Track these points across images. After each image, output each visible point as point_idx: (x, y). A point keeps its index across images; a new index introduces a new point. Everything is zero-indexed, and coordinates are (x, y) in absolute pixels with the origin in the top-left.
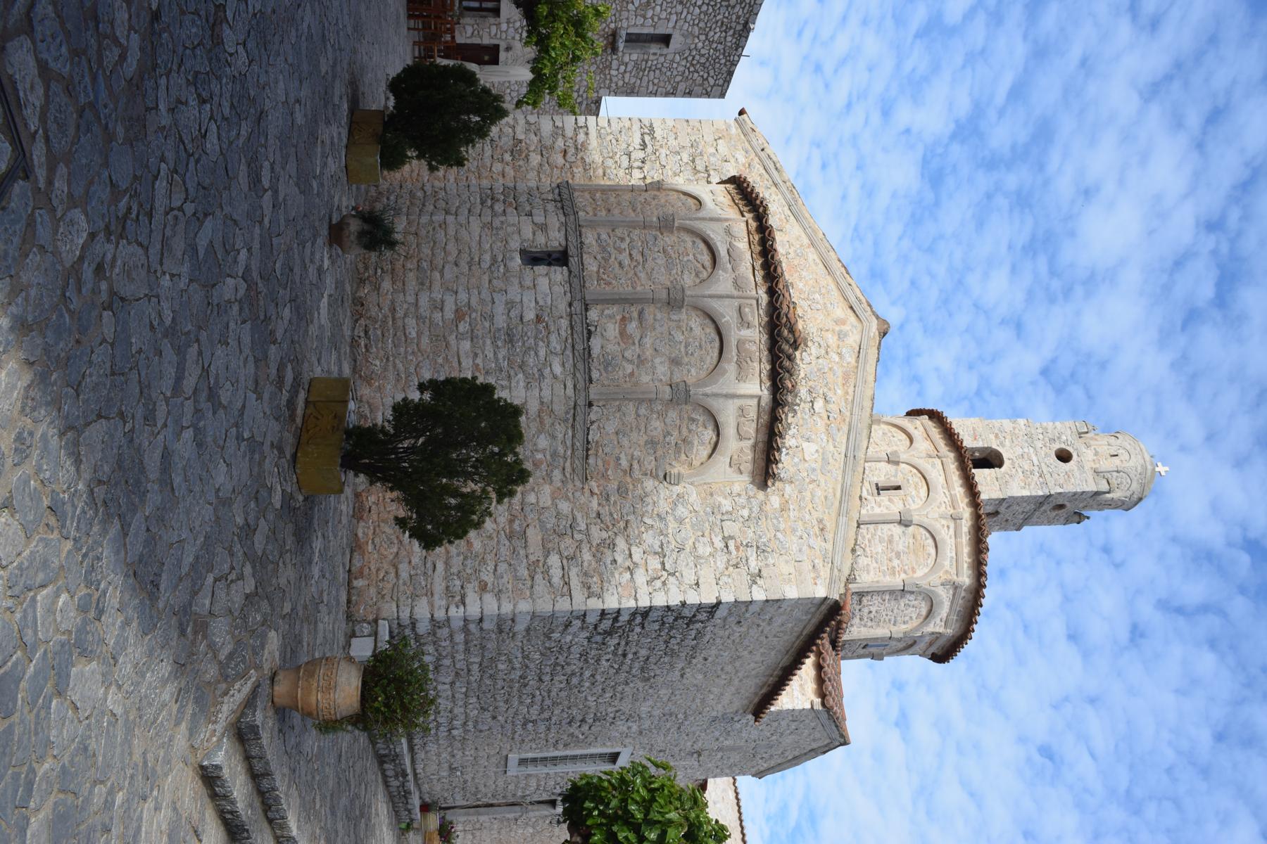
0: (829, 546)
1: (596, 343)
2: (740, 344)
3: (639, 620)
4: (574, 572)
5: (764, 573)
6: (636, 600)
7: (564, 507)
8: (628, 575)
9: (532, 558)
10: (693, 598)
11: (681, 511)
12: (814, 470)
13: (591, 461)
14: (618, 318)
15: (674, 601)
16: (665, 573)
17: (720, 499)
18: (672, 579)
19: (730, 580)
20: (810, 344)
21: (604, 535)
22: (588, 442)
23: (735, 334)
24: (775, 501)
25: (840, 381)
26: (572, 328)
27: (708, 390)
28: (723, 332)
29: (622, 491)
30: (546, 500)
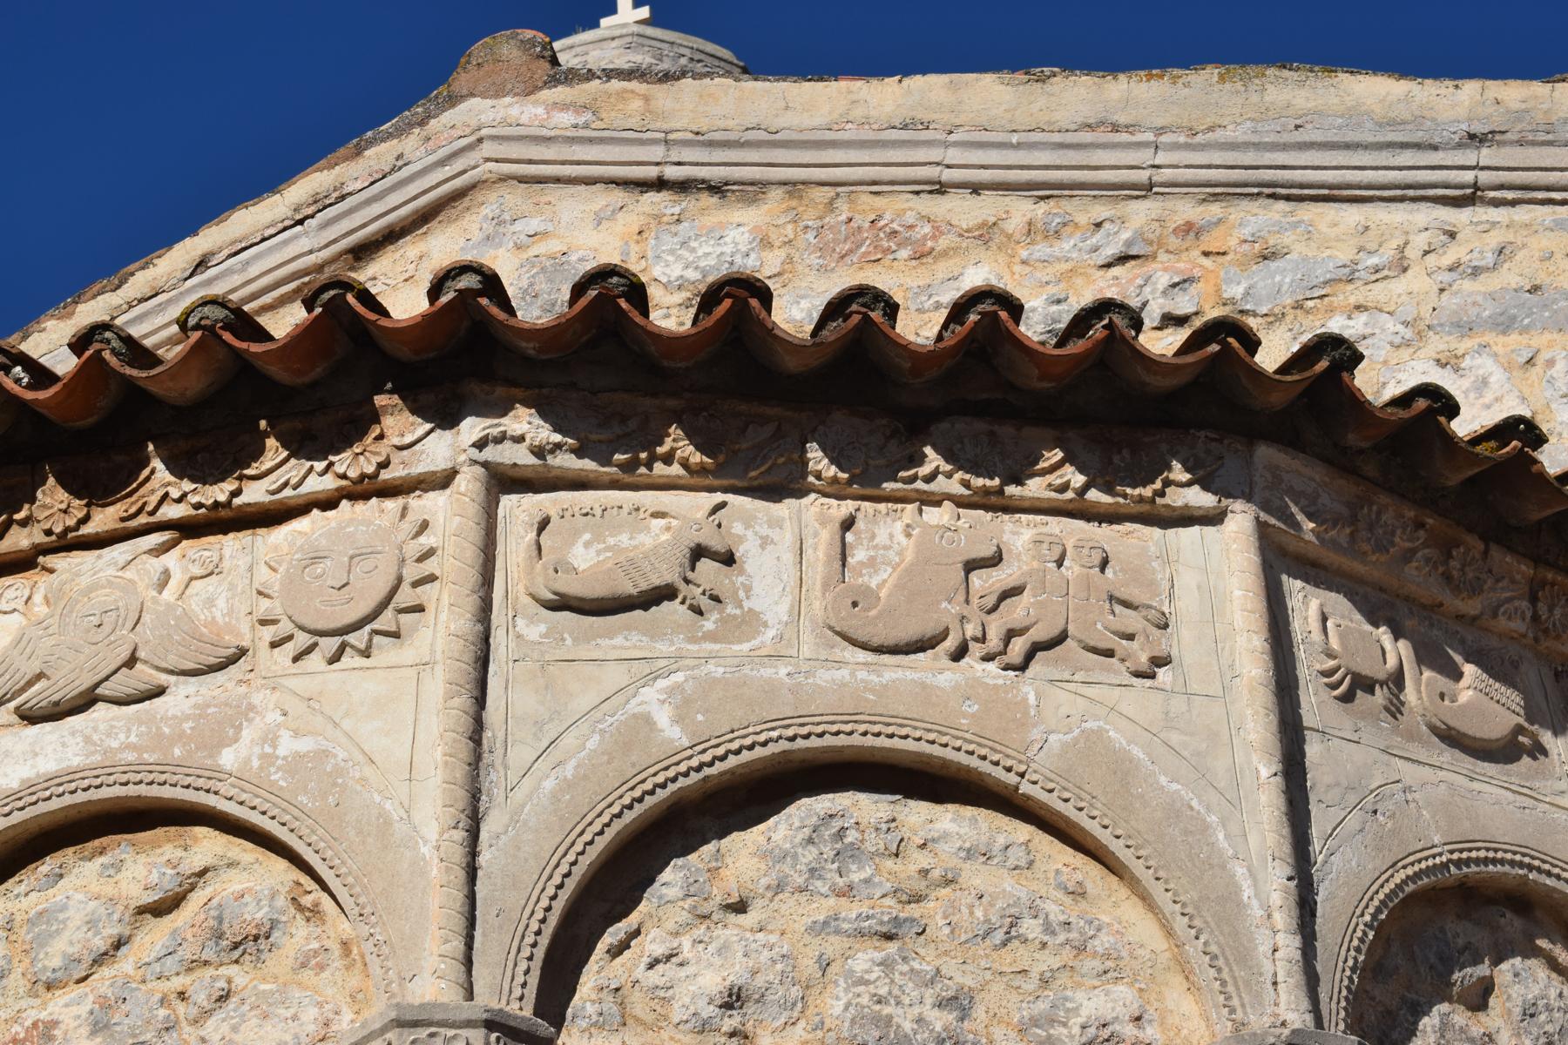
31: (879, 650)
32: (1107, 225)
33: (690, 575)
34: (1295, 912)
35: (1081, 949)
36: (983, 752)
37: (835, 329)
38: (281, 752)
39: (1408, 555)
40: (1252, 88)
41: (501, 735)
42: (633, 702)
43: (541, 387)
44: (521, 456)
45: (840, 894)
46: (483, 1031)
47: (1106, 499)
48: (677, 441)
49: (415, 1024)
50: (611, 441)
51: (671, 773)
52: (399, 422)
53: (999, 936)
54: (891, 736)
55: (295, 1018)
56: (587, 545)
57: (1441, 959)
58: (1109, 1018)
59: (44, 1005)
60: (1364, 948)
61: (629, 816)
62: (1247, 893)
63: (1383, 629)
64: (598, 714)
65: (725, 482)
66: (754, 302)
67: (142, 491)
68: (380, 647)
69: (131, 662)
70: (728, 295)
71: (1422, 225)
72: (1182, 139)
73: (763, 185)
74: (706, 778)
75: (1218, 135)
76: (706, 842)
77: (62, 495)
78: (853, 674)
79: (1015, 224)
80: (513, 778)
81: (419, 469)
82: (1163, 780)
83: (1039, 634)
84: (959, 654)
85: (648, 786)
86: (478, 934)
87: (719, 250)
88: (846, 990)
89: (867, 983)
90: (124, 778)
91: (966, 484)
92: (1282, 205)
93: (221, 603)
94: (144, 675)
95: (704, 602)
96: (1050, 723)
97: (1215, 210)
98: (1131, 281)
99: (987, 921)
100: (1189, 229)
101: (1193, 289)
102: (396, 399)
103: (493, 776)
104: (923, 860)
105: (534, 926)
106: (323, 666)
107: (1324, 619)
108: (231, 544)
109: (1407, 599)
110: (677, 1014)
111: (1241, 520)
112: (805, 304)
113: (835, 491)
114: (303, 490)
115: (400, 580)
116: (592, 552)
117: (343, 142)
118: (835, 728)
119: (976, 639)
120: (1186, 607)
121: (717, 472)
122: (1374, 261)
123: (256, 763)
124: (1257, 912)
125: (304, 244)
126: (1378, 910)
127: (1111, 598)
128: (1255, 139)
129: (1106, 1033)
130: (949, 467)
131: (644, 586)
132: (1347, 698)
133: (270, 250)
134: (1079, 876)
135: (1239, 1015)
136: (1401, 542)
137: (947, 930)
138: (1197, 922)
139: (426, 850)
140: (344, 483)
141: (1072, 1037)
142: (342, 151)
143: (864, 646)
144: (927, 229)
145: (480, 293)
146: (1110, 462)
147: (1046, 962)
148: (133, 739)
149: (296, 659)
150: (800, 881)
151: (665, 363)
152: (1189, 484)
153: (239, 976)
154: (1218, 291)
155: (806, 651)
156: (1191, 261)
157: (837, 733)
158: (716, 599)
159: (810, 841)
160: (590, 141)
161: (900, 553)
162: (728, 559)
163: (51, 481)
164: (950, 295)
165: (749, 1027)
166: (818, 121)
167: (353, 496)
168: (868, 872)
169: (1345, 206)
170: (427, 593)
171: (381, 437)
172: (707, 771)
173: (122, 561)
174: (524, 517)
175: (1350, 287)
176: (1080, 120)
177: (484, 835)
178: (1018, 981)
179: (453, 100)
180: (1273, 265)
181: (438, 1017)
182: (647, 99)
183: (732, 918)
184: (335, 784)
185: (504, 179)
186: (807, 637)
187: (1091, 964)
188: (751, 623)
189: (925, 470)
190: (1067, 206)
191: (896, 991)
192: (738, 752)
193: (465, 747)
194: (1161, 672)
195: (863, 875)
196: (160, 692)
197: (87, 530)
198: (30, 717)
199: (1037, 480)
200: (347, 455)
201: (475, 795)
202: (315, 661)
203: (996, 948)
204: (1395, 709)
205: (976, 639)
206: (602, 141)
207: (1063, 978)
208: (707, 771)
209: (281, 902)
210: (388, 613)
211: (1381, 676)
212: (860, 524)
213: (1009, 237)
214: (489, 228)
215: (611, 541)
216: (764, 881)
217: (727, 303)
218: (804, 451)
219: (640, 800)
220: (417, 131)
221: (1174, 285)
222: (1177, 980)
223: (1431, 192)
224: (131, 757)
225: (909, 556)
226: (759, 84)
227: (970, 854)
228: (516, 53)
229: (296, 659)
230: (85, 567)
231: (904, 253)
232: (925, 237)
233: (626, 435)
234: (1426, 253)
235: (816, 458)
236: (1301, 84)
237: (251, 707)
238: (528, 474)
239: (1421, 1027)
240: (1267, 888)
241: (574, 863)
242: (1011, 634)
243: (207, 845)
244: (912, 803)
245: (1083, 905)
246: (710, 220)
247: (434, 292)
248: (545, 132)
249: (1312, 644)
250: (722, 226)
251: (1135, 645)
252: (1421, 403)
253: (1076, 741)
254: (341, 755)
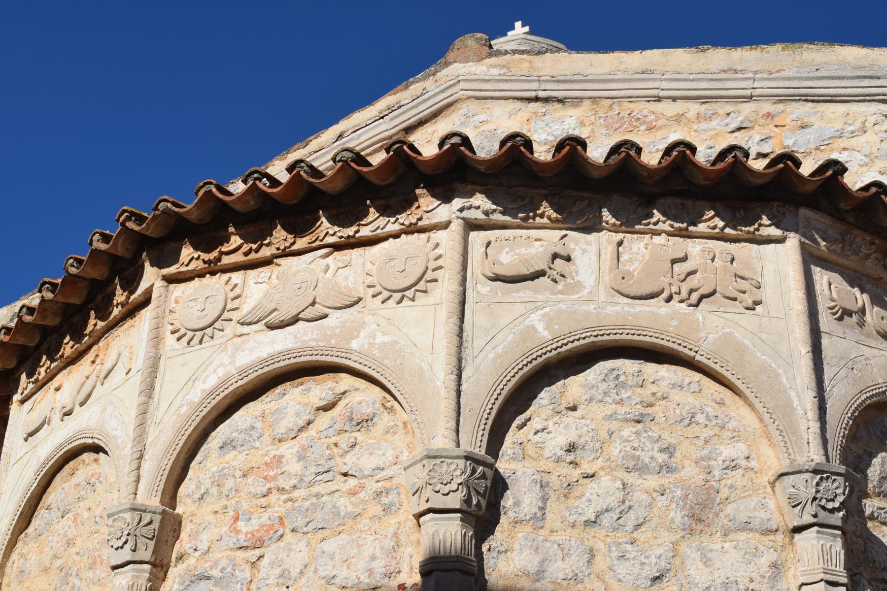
31: (634, 298)
32: (732, 114)
33: (552, 266)
34: (817, 412)
35: (722, 428)
36: (679, 342)
37: (615, 159)
38: (377, 341)
39: (867, 257)
40: (797, 53)
41: (470, 335)
42: (527, 320)
43: (487, 185)
44: (478, 215)
45: (617, 403)
46: (464, 460)
47: (733, 232)
48: (545, 208)
49: (435, 457)
50: (517, 208)
51: (544, 351)
52: (426, 201)
53: (687, 422)
54: (639, 335)
55: (384, 454)
56: (507, 253)
57: (882, 433)
58: (735, 457)
59: (278, 448)
60: (848, 428)
61: (526, 369)
62: (796, 403)
63: (856, 289)
64: (512, 326)
65: (567, 226)
66: (579, 148)
67: (317, 231)
68: (419, 297)
69: (313, 303)
70: (568, 145)
71: (873, 112)
72: (765, 76)
73: (581, 99)
74: (559, 353)
75: (782, 74)
76: (559, 380)
77: (284, 233)
78: (622, 308)
79: (692, 114)
80: (476, 353)
81: (434, 221)
82: (759, 354)
83: (704, 290)
84: (669, 300)
85: (534, 356)
86: (461, 419)
87: (562, 127)
88: (620, 444)
89: (629, 441)
90: (311, 353)
91: (672, 226)
92: (810, 104)
93: (351, 279)
94: (318, 310)
95: (558, 277)
96: (707, 330)
97: (780, 107)
98: (742, 138)
99: (682, 415)
100: (768, 115)
101: (770, 142)
102: (425, 191)
103: (467, 352)
104: (654, 389)
105: (485, 416)
106: (395, 305)
107: (830, 284)
108: (355, 253)
109: (867, 276)
110: (547, 454)
111: (793, 241)
112: (600, 150)
113: (615, 229)
114: (385, 230)
115: (427, 268)
116: (509, 256)
117: (400, 83)
118: (614, 332)
119: (676, 293)
120: (768, 279)
121: (563, 221)
122: (851, 128)
123: (366, 346)
124: (801, 412)
125: (384, 127)
126: (854, 412)
127: (736, 275)
128: (798, 75)
129: (733, 464)
130: (664, 219)
131: (532, 270)
132: (840, 319)
133: (369, 130)
134: (722, 396)
135: (792, 457)
136: (864, 251)
137: (664, 419)
138: (773, 416)
139: (439, 383)
140: (403, 227)
141: (718, 465)
142: (400, 87)
143: (627, 296)
144: (653, 117)
145: (461, 145)
146: (735, 216)
147: (707, 433)
148: (314, 336)
149: (383, 302)
150: (600, 397)
151: (541, 175)
152: (770, 225)
153: (360, 437)
154: (782, 142)
155: (602, 298)
156: (770, 130)
157: (616, 334)
158: (563, 276)
159: (604, 380)
160: (506, 81)
161: (643, 256)
162: (568, 259)
163: (279, 227)
164: (663, 146)
165: (578, 460)
166: (605, 71)
167: (407, 233)
168: (629, 394)
169: (838, 104)
170: (439, 274)
171: (418, 207)
172: (559, 350)
173: (309, 260)
174: (480, 241)
175: (841, 140)
176: (720, 68)
177: (463, 377)
178: (695, 441)
179: (447, 64)
180: (806, 131)
181: (444, 454)
182: (530, 62)
183: (570, 413)
184: (400, 355)
185: (469, 98)
186: (602, 292)
187: (727, 434)
188: (578, 286)
189: (654, 220)
190: (714, 106)
191: (642, 445)
192: (573, 342)
193: (456, 339)
194: (757, 307)
195: (627, 395)
196: (325, 316)
197: (294, 248)
198: (271, 327)
199: (703, 224)
200: (404, 215)
201: (460, 360)
202: (391, 303)
203: (685, 427)
204: (862, 324)
205: (676, 293)
206: (511, 81)
207: (715, 440)
208: (559, 350)
209: (378, 405)
210: (422, 282)
211: (855, 309)
212: (625, 244)
213: (689, 120)
214: (463, 119)
215: (517, 251)
216: (584, 397)
217: (567, 148)
218: (601, 212)
219: (531, 362)
220: (431, 78)
221: (762, 140)
222: (765, 441)
223: (877, 98)
224: (313, 344)
225: (647, 257)
226: (579, 55)
227: (674, 386)
228: (474, 43)
229: (383, 302)
230: (294, 264)
231: (643, 128)
232: (652, 121)
233: (524, 205)
234: (875, 124)
235: (606, 215)
236: (819, 51)
237: (364, 323)
238: (482, 223)
239: (873, 462)
240: (804, 401)
241: (502, 389)
242: (691, 291)
243: (346, 381)
244: (648, 364)
245: (723, 408)
246: (558, 114)
247: (441, 145)
248: (487, 78)
249: (825, 295)
250: (563, 117)
251: (746, 295)
252: (874, 190)
253: (720, 337)
254: (403, 343)
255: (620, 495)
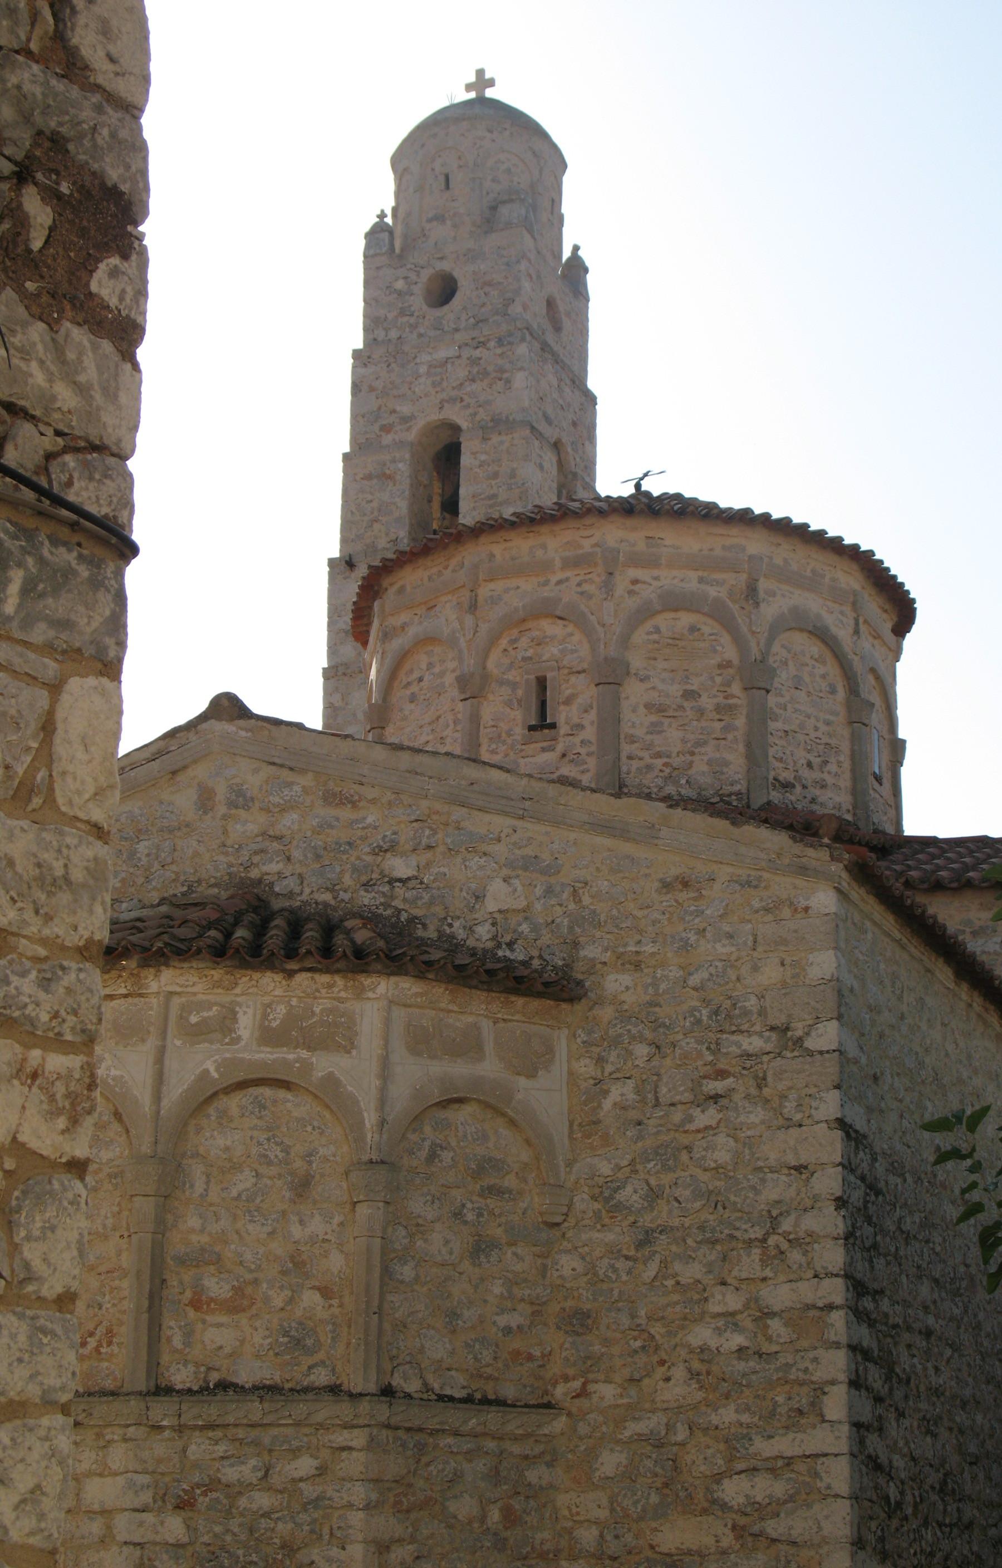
0: (724, 872)
1: (248, 1372)
2: (269, 1036)
3: (867, 1303)
4: (764, 1448)
5: (778, 1019)
6: (830, 1307)
7: (610, 1462)
8: (775, 1325)
9: (728, 1540)
10: (829, 1182)
11: (630, 1194)
12: (549, 891)
13: (509, 1392)
14: (191, 1313)
15: (830, 1222)
16: (772, 1240)
17: (607, 1104)
18: (786, 1225)
19: (793, 1095)
20: (254, 874)
21: (679, 1373)
22: (468, 1400)
23: (249, 1049)
24: (616, 982)
25: (346, 814)
26: (212, 1427)
27: (370, 1119)
28: (241, 1076)
29: (579, 1321)
30: (594, 1505)
188: (239, 1038)
255: (254, 1180)
